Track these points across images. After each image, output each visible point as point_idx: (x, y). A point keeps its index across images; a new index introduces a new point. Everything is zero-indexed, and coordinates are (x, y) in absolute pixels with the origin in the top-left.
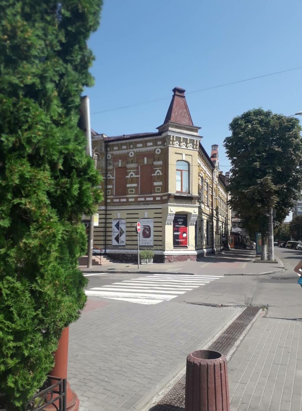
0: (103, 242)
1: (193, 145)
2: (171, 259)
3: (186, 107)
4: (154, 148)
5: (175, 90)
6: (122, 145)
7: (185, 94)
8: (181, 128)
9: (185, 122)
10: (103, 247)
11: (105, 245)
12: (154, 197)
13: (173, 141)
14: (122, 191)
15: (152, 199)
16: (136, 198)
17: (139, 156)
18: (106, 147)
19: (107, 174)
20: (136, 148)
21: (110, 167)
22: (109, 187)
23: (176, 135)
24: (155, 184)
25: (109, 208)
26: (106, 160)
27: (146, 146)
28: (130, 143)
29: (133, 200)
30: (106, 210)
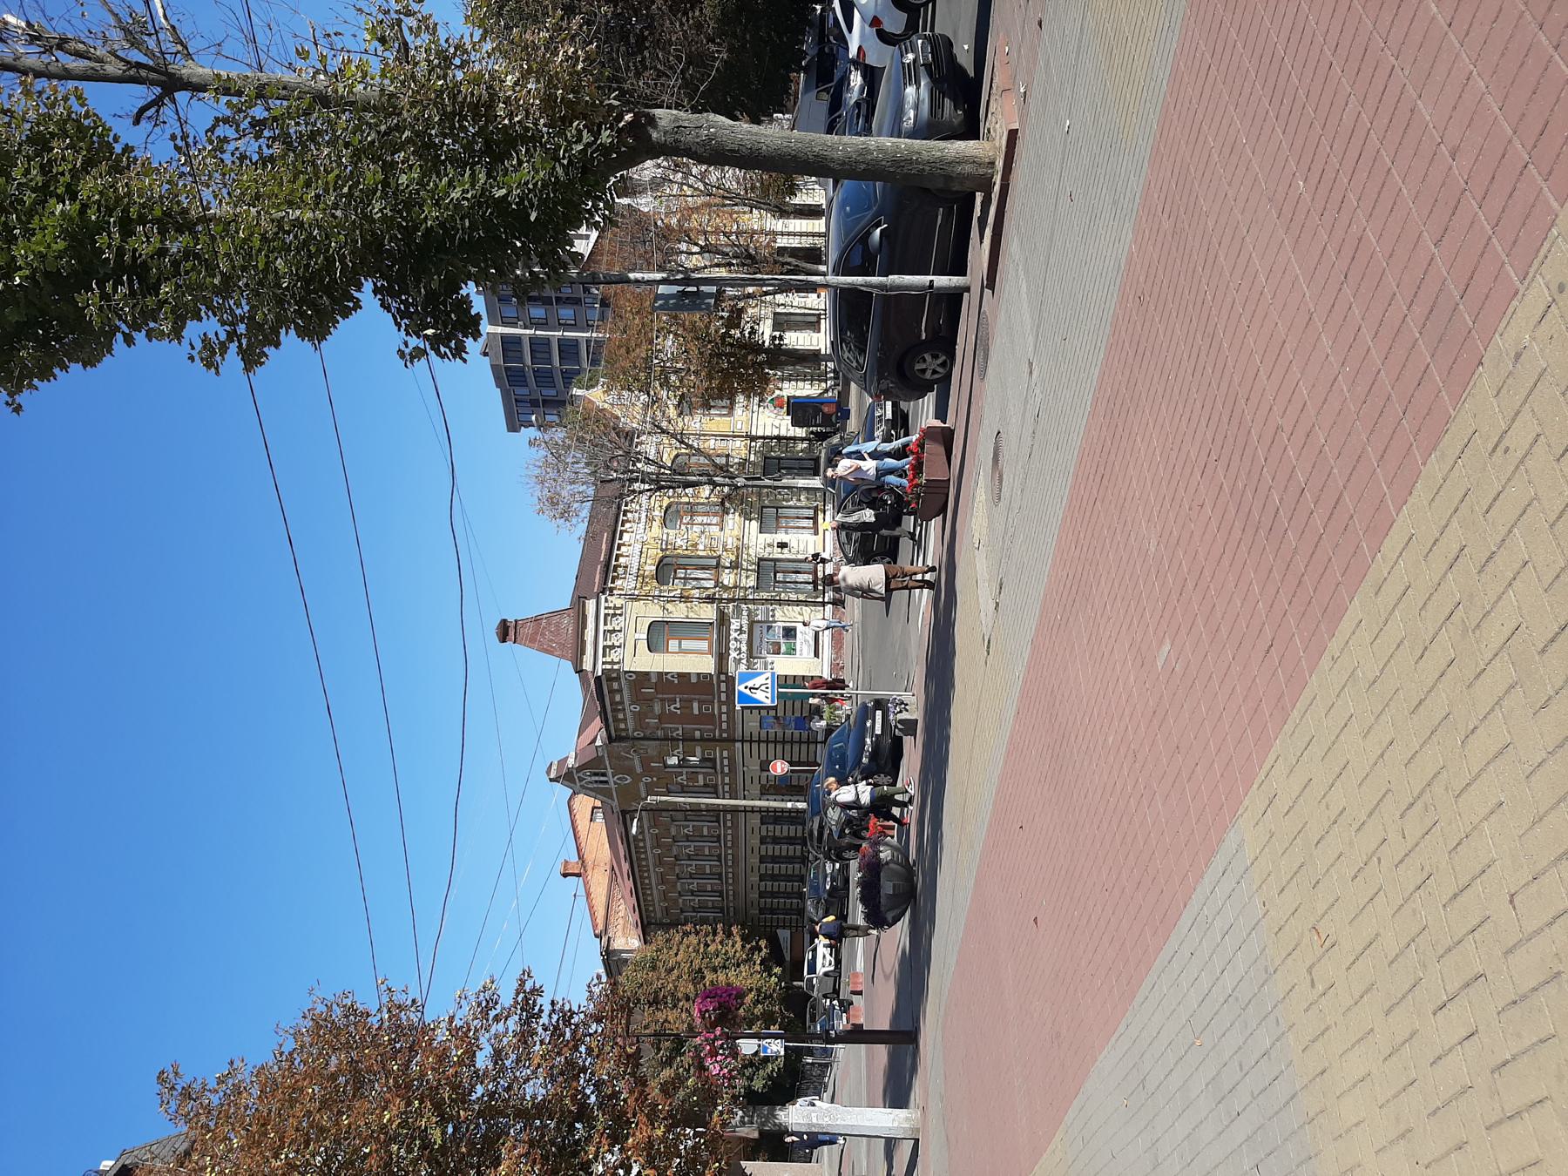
0: (804, 747)
1: (614, 615)
2: (835, 667)
3: (537, 619)
4: (623, 681)
5: (503, 638)
6: (616, 720)
7: (511, 619)
8: (583, 642)
9: (567, 623)
10: (812, 747)
11: (808, 743)
12: (719, 682)
13: (612, 663)
14: (710, 718)
15: (723, 686)
16: (721, 703)
17: (637, 698)
18: (620, 739)
19: (673, 739)
20: (622, 703)
21: (660, 733)
22: (698, 734)
23: (600, 659)
24: (694, 680)
25: (739, 734)
26: (644, 739)
27: (620, 691)
28: (613, 711)
29: (724, 709)
30: (743, 741)
